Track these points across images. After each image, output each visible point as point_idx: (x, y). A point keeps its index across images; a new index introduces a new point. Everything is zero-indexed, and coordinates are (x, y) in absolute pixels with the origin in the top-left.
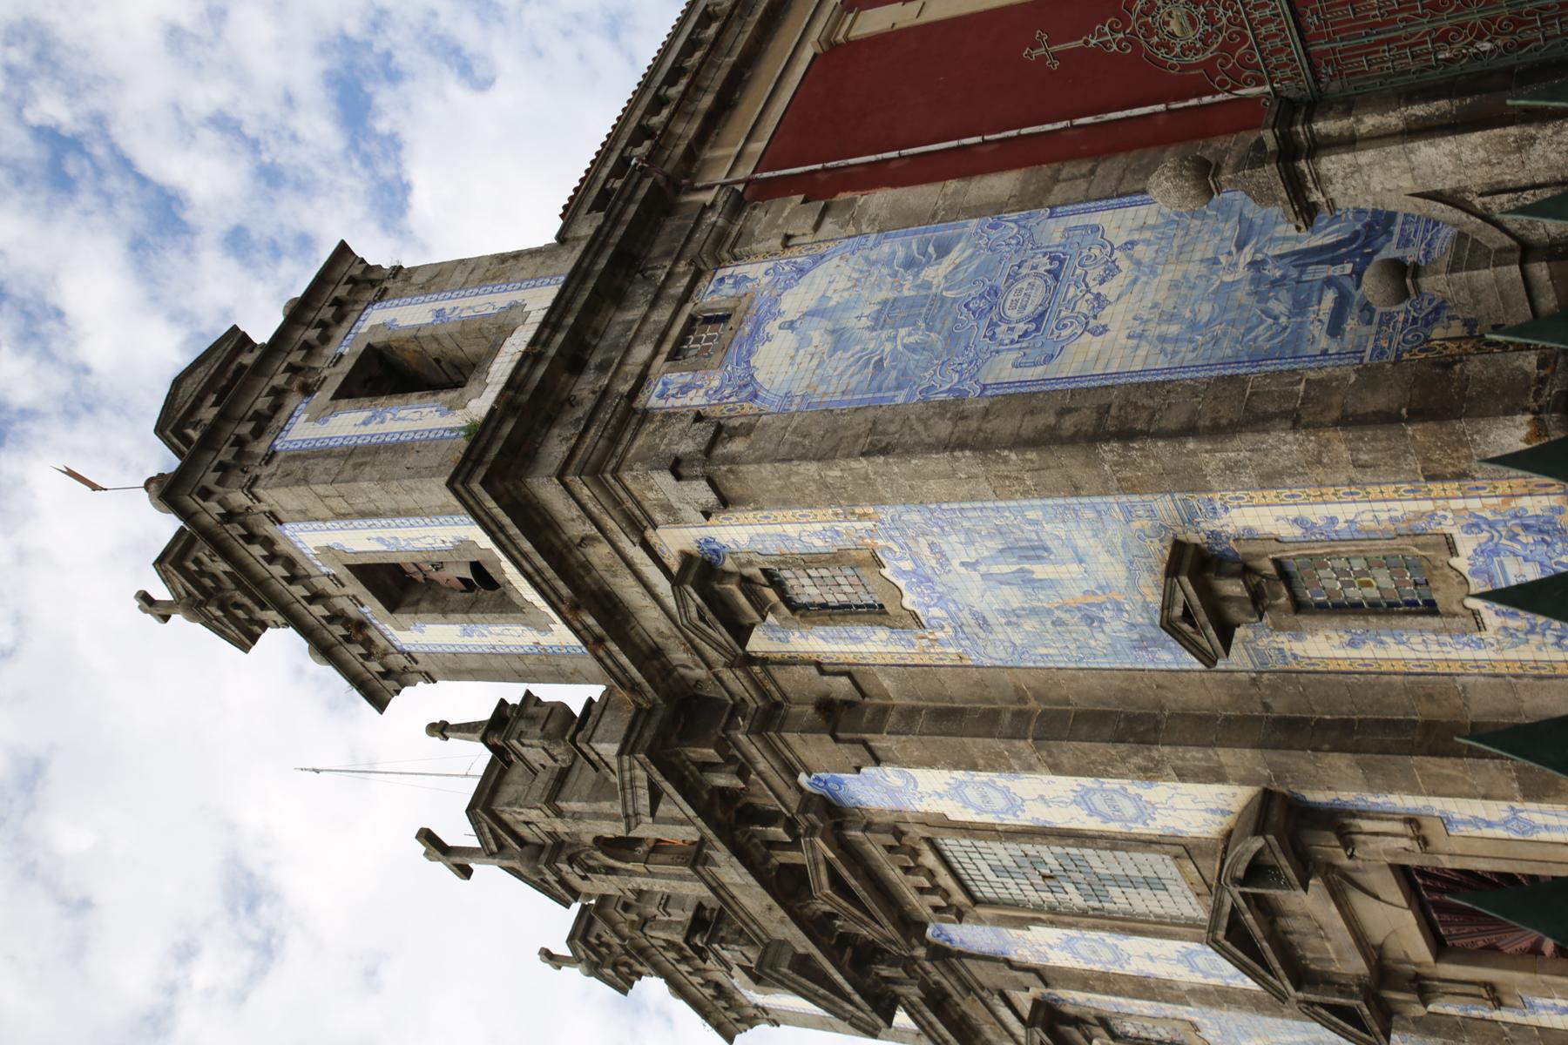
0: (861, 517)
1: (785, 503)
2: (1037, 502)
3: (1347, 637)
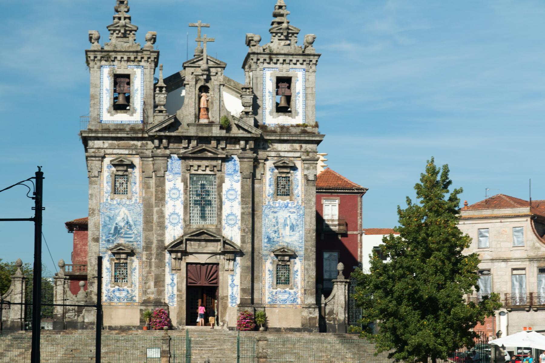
1: (306, 191)
2: (304, 234)
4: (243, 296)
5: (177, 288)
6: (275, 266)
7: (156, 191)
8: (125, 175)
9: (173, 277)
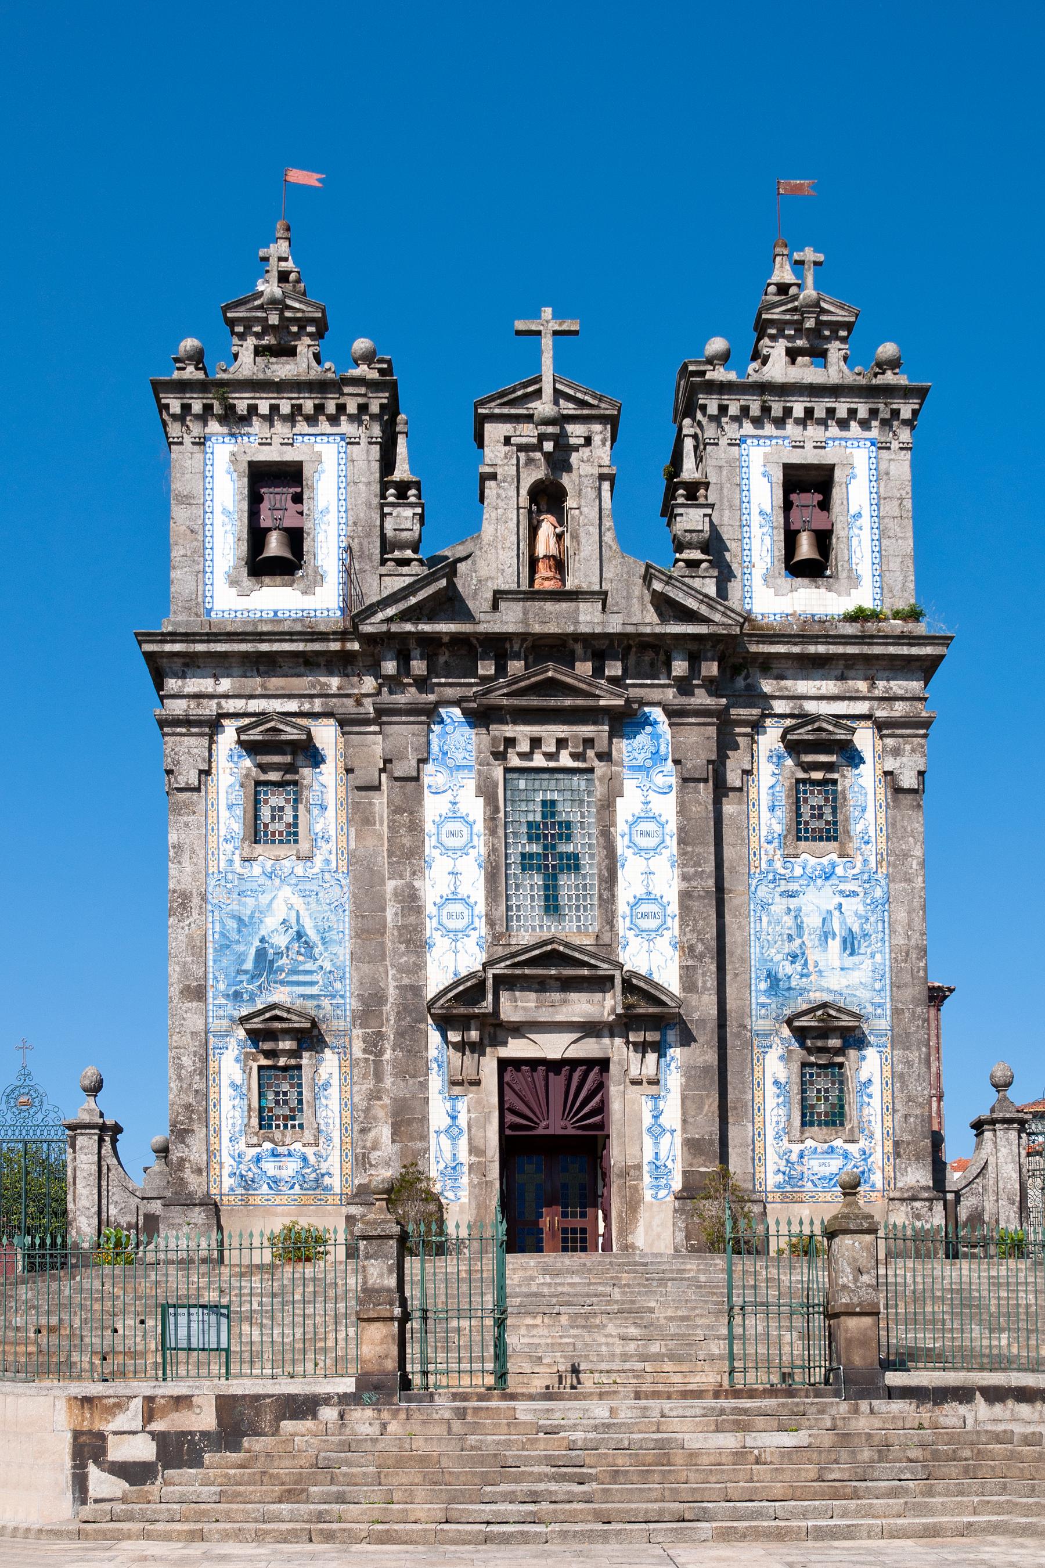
0: (878, 863)
1: (891, 824)
2: (887, 963)
3: (783, 1080)
4: (691, 1165)
5: (470, 1143)
6: (796, 1067)
8: (288, 783)
9: (453, 1107)
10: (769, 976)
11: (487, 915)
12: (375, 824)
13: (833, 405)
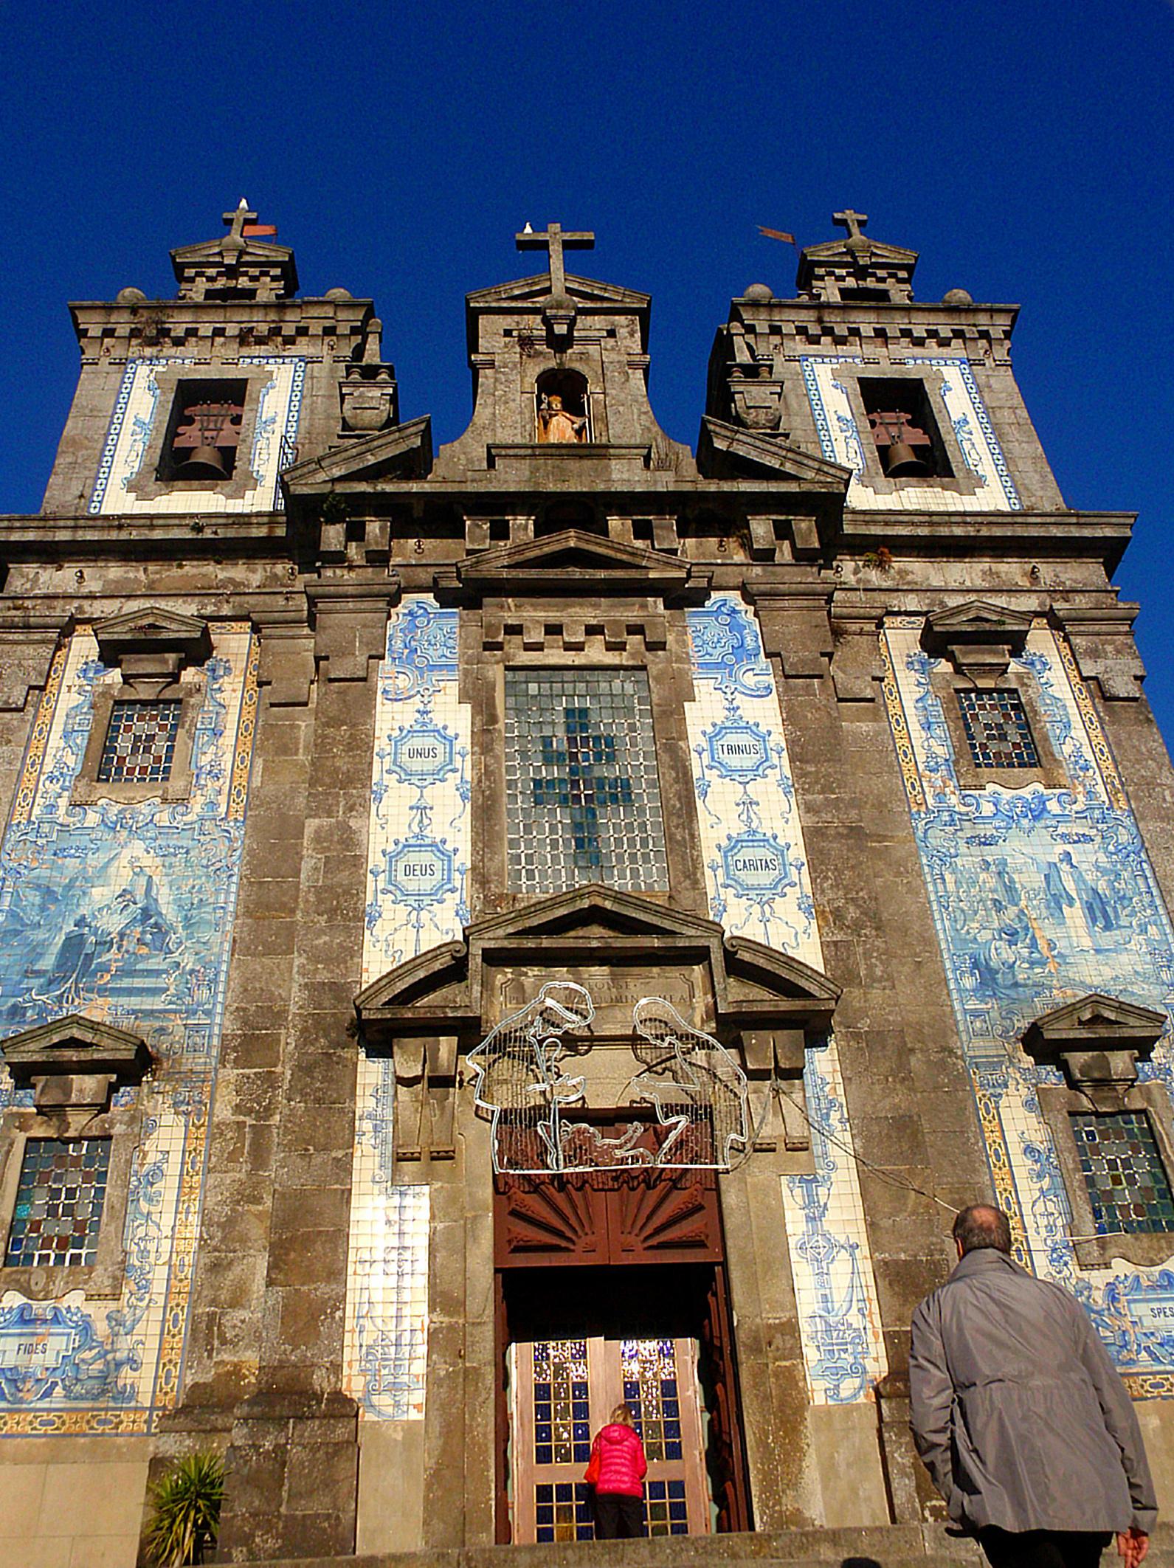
1: (1114, 745)
3: (1041, 1147)
4: (900, 1319)
6: (1061, 1120)
7: (321, 745)
8: (167, 702)
10: (976, 965)
11: (474, 868)
12: (296, 754)
13: (908, 327)
